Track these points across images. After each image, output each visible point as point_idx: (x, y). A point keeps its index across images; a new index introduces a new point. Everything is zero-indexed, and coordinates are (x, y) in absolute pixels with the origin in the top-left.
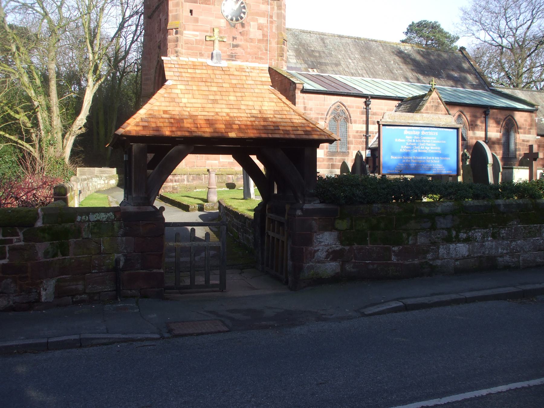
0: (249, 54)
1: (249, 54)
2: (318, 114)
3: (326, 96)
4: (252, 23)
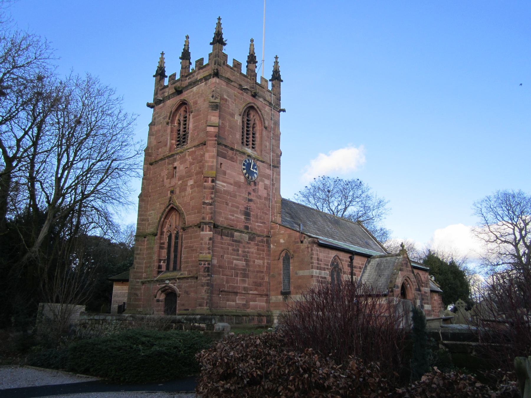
0: (258, 208)
1: (258, 208)
2: (325, 264)
3: (327, 250)
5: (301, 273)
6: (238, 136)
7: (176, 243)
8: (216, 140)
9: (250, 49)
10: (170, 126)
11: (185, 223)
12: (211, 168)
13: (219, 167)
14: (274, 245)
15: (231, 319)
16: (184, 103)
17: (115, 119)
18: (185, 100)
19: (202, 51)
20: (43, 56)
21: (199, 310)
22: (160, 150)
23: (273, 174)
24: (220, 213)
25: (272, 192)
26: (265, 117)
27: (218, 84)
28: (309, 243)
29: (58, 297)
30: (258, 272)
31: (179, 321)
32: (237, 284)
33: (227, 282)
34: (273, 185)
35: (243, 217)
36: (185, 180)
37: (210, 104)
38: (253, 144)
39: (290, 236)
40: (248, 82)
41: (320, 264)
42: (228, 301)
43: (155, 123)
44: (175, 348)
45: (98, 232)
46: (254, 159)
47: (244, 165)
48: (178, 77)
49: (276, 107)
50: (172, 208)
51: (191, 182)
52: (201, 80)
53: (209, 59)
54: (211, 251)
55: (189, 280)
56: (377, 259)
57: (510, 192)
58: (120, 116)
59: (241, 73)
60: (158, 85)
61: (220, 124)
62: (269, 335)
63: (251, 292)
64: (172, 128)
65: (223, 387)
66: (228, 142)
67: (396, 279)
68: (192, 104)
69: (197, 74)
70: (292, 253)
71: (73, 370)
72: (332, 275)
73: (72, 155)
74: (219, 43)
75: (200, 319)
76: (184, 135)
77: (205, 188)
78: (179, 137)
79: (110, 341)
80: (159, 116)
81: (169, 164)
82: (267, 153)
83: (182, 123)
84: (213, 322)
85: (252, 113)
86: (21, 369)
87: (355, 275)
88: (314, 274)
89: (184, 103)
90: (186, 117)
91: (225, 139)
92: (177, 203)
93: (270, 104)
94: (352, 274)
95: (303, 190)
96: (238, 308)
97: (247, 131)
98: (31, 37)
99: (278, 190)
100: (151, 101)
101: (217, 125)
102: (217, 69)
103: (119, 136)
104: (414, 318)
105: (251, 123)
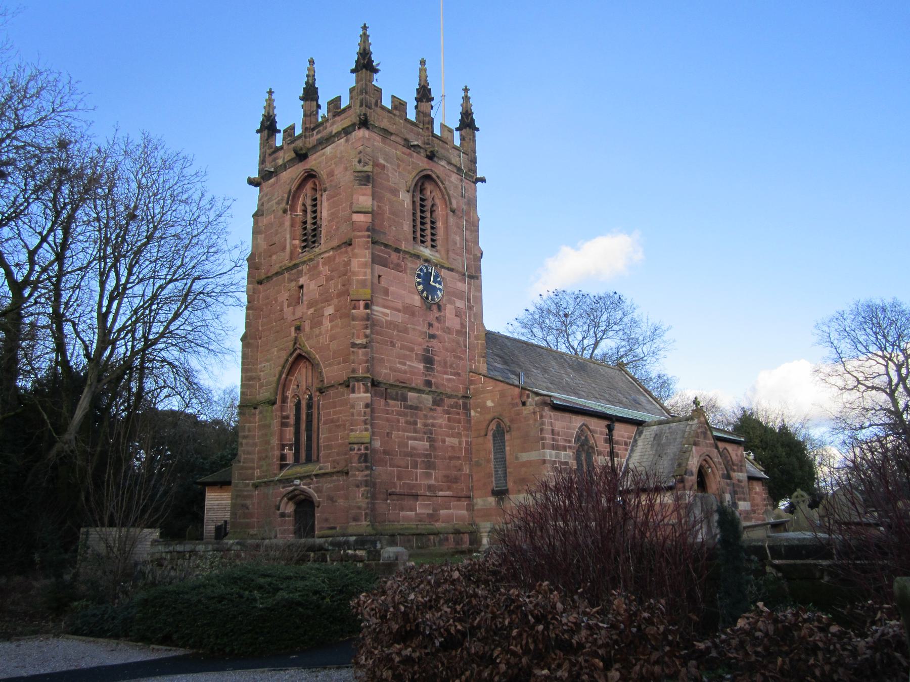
0: (447, 350)
1: (447, 350)
2: (566, 440)
3: (567, 415)
4: (448, 306)
5: (525, 457)
6: (407, 227)
7: (309, 416)
8: (369, 237)
9: (420, 77)
10: (289, 216)
11: (322, 381)
12: (363, 284)
13: (376, 281)
14: (476, 412)
15: (409, 541)
16: (310, 176)
17: (195, 209)
18: (312, 170)
19: (337, 84)
20: (66, 107)
21: (353, 527)
22: (274, 257)
23: (469, 289)
24: (382, 361)
25: (470, 320)
26: (451, 192)
27: (369, 139)
28: (536, 405)
29: (112, 516)
30: (451, 458)
31: (321, 548)
32: (416, 480)
33: (400, 478)
34: (470, 308)
35: (421, 366)
36: (319, 307)
37: (356, 174)
38: (433, 240)
39: (503, 395)
40: (418, 134)
41: (557, 441)
42: (402, 509)
43: (263, 211)
44: (316, 593)
45: (174, 404)
46: (436, 265)
47: (419, 276)
48: (298, 131)
49: (471, 176)
50: (300, 357)
51: (329, 310)
52: (338, 134)
53: (351, 98)
54: (369, 426)
55: (335, 478)
56: (655, 427)
57: (878, 302)
58: (202, 203)
59: (407, 120)
60: (265, 146)
61: (375, 209)
62: (475, 564)
63: (441, 493)
64: (292, 220)
65: (399, 653)
66: (390, 239)
67: (688, 459)
68: (325, 177)
69: (332, 124)
70: (508, 424)
71: (145, 639)
72: (578, 458)
73: (124, 272)
74: (367, 69)
75: (356, 541)
76: (314, 230)
77: (354, 319)
78: (305, 235)
79: (204, 586)
80: (269, 200)
81: (290, 281)
82: (457, 254)
83: (309, 209)
84: (379, 546)
85: (429, 187)
86: (55, 640)
87: (617, 457)
88: (548, 458)
89: (310, 176)
90: (315, 200)
91: (385, 233)
92: (308, 346)
93: (459, 169)
94: (612, 454)
95: (522, 314)
96: (420, 521)
97: (422, 218)
98: (45, 75)
99: (479, 316)
100: (255, 175)
101: (370, 210)
102: (365, 115)
103: (202, 237)
104: (721, 523)
105: (428, 204)
